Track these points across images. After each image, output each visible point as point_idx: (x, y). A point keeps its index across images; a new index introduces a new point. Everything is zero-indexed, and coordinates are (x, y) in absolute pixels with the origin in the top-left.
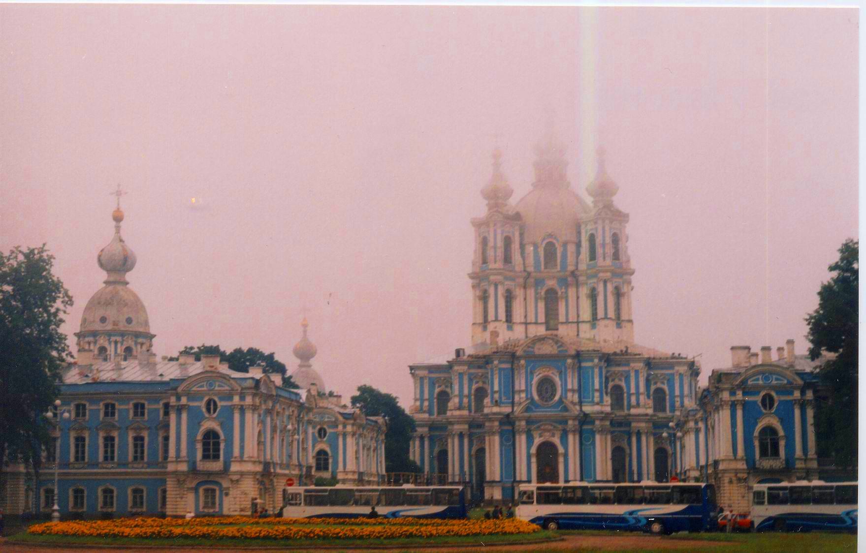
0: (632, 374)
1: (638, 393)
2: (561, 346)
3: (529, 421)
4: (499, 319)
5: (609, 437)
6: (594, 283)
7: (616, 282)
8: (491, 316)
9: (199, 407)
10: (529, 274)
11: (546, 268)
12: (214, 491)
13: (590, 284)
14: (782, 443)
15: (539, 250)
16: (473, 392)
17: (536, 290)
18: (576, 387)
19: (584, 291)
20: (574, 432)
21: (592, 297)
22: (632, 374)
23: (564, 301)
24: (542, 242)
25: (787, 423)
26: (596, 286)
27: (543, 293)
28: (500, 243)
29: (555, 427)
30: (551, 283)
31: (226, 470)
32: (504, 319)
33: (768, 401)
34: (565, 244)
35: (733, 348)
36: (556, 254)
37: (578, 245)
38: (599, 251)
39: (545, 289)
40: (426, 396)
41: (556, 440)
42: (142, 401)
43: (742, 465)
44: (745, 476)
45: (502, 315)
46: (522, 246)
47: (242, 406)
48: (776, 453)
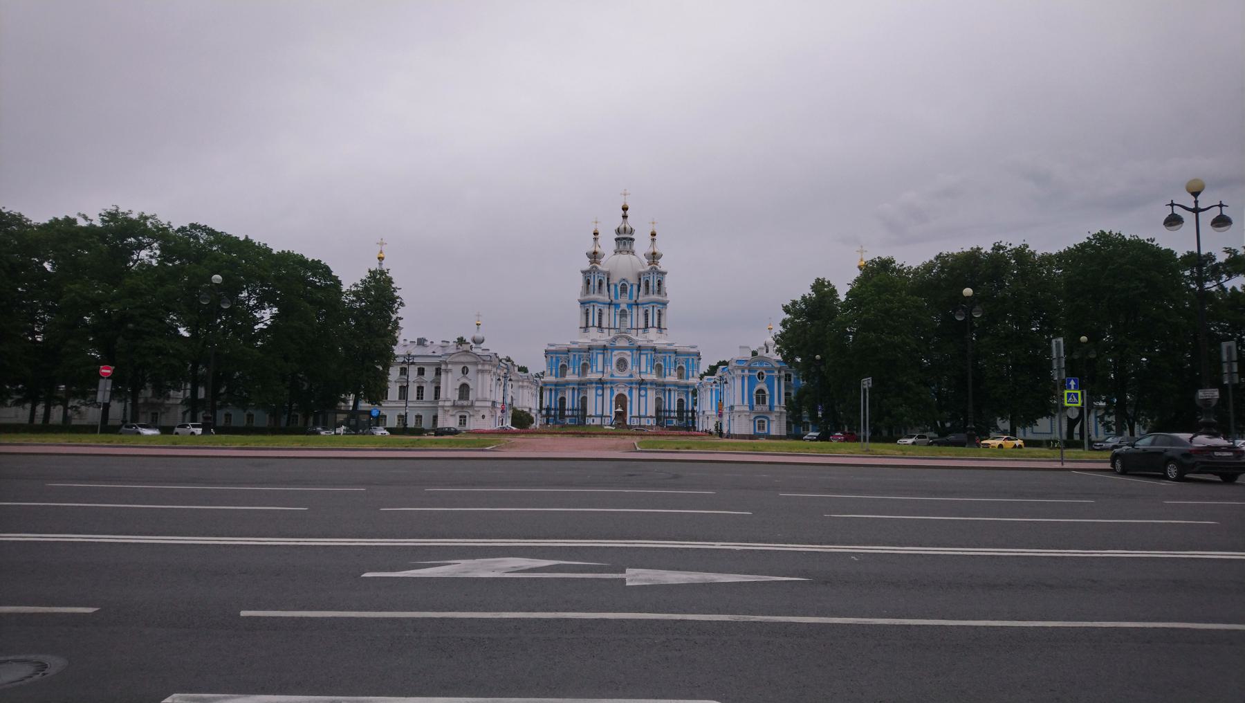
1: (670, 369)
3: (612, 382)
5: (654, 392)
9: (755, 376)
12: (465, 417)
14: (767, 398)
19: (641, 311)
25: (771, 387)
27: (619, 311)
30: (624, 306)
31: (472, 406)
33: (760, 376)
34: (632, 286)
35: (740, 347)
37: (639, 286)
38: (651, 289)
39: (620, 309)
41: (626, 393)
42: (790, 373)
43: (747, 409)
44: (748, 414)
46: (608, 285)
47: (743, 376)
48: (764, 402)
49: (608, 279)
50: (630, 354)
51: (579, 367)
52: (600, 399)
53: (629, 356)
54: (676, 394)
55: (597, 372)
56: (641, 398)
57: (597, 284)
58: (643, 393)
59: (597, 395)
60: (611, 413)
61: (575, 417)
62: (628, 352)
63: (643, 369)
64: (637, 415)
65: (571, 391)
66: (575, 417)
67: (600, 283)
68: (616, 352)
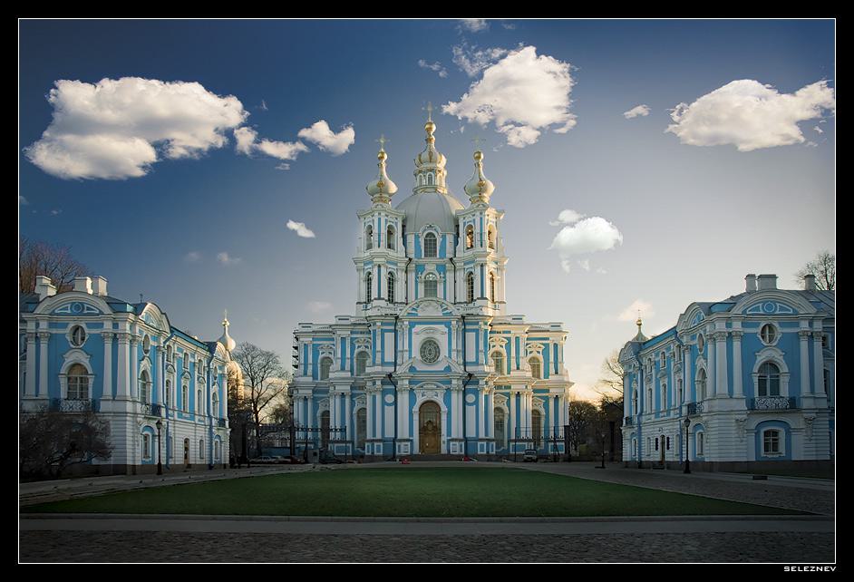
0: (513, 341)
1: (517, 358)
2: (446, 309)
8: (374, 295)
10: (410, 259)
16: (355, 355)
17: (417, 274)
18: (460, 348)
19: (461, 276)
20: (458, 391)
22: (513, 341)
26: (473, 270)
28: (384, 231)
32: (387, 298)
40: (310, 361)
41: (440, 400)
45: (385, 294)
46: (404, 236)
49: (404, 226)
51: (352, 359)
52: (390, 410)
53: (443, 333)
55: (383, 364)
58: (471, 398)
59: (384, 403)
60: (411, 433)
61: (349, 442)
62: (442, 328)
63: (471, 357)
65: (338, 400)
66: (349, 442)
68: (418, 328)
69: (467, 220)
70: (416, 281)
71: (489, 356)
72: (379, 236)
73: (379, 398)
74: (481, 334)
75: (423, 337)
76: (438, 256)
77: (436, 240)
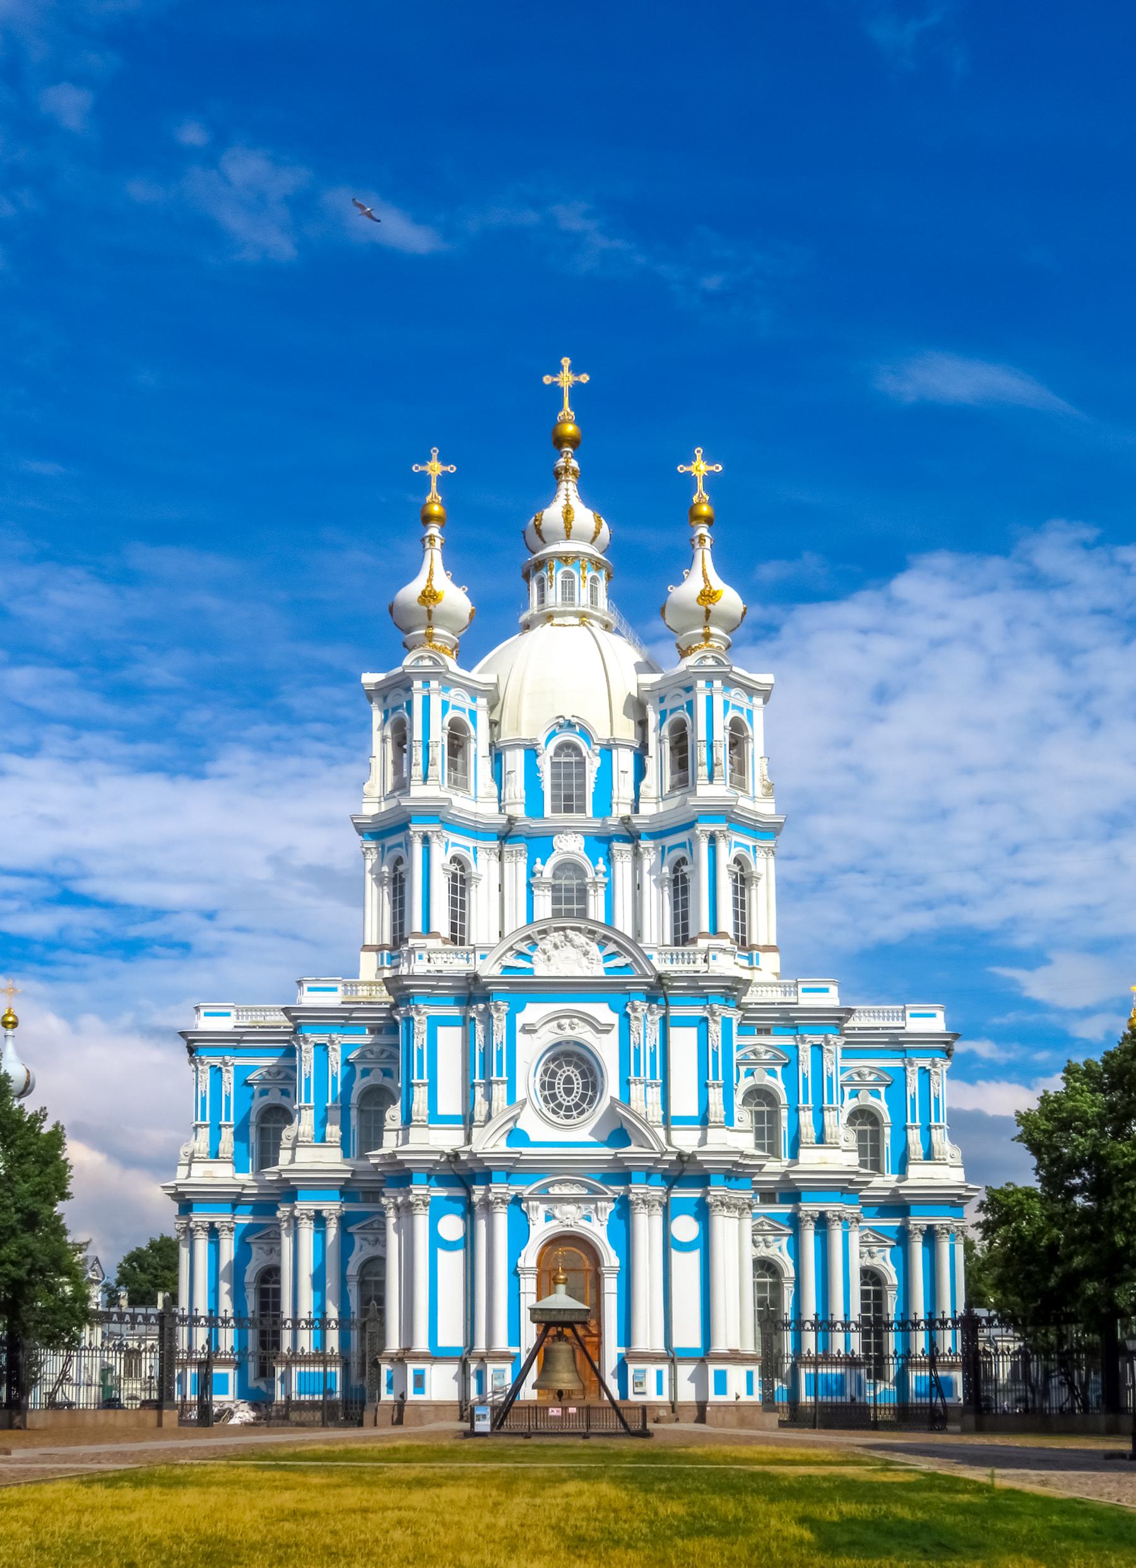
2: (614, 954)
4: (434, 928)
6: (682, 845)
7: (737, 844)
10: (511, 820)
11: (552, 812)
13: (671, 848)
15: (539, 761)
16: (354, 1099)
17: (531, 863)
21: (675, 882)
23: (601, 892)
24: (547, 744)
29: (593, 1190)
34: (608, 749)
36: (582, 776)
37: (641, 754)
39: (552, 861)
41: (598, 1231)
46: (497, 755)
49: (494, 724)
50: (614, 1018)
52: (451, 1264)
53: (605, 1030)
54: (855, 1237)
55: (435, 1118)
56: (675, 1255)
57: (439, 735)
59: (437, 1242)
62: (602, 1012)
63: (685, 1103)
64: (659, 1347)
67: (457, 742)
69: (668, 705)
70: (529, 886)
71: (738, 1099)
72: (427, 748)
73: (422, 1222)
74: (715, 1029)
75: (547, 1036)
76: (589, 812)
77: (582, 764)
